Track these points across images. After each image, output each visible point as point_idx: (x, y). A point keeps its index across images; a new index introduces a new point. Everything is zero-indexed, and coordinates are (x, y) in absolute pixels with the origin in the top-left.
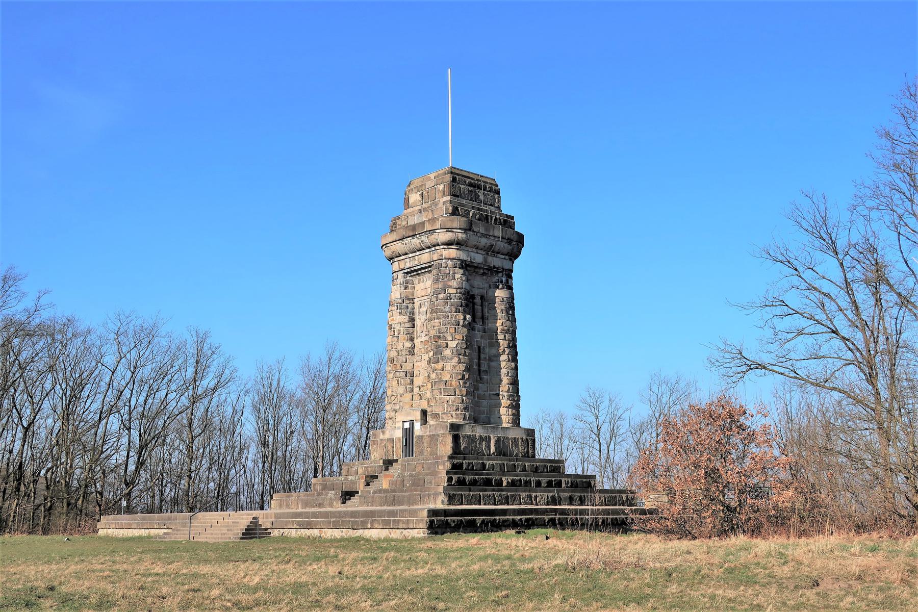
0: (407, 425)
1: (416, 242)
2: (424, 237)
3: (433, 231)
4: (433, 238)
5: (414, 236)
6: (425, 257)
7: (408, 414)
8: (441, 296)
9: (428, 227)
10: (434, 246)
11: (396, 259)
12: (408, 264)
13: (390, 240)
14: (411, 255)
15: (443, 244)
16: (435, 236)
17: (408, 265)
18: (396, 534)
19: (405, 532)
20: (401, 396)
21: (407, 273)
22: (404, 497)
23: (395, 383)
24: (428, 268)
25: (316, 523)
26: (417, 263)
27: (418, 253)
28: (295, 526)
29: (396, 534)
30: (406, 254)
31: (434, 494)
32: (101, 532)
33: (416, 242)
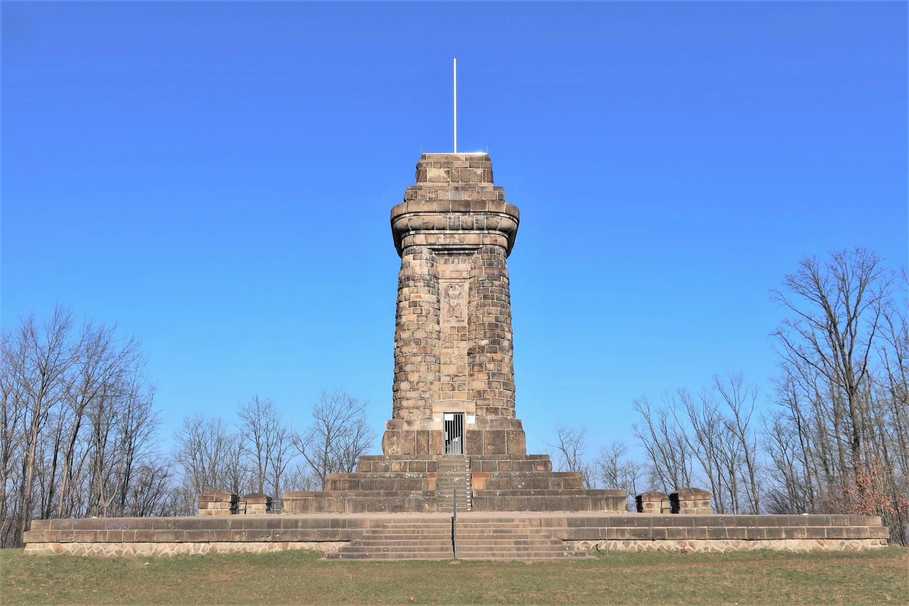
0: (450, 418)
1: (468, 219)
2: (481, 217)
3: (497, 214)
4: (494, 221)
5: (464, 213)
6: (472, 238)
7: (453, 405)
8: (497, 283)
9: (490, 207)
10: (488, 229)
11: (422, 232)
12: (442, 240)
13: (426, 209)
14: (448, 232)
15: (500, 230)
16: (497, 219)
17: (442, 240)
18: (834, 545)
19: (847, 543)
20: (431, 383)
21: (434, 250)
22: (562, 500)
23: (423, 368)
24: (467, 251)
25: (678, 532)
26: (457, 241)
27: (460, 232)
28: (627, 536)
29: (834, 545)
30: (444, 229)
31: (613, 498)
32: (32, 548)
33: (468, 219)
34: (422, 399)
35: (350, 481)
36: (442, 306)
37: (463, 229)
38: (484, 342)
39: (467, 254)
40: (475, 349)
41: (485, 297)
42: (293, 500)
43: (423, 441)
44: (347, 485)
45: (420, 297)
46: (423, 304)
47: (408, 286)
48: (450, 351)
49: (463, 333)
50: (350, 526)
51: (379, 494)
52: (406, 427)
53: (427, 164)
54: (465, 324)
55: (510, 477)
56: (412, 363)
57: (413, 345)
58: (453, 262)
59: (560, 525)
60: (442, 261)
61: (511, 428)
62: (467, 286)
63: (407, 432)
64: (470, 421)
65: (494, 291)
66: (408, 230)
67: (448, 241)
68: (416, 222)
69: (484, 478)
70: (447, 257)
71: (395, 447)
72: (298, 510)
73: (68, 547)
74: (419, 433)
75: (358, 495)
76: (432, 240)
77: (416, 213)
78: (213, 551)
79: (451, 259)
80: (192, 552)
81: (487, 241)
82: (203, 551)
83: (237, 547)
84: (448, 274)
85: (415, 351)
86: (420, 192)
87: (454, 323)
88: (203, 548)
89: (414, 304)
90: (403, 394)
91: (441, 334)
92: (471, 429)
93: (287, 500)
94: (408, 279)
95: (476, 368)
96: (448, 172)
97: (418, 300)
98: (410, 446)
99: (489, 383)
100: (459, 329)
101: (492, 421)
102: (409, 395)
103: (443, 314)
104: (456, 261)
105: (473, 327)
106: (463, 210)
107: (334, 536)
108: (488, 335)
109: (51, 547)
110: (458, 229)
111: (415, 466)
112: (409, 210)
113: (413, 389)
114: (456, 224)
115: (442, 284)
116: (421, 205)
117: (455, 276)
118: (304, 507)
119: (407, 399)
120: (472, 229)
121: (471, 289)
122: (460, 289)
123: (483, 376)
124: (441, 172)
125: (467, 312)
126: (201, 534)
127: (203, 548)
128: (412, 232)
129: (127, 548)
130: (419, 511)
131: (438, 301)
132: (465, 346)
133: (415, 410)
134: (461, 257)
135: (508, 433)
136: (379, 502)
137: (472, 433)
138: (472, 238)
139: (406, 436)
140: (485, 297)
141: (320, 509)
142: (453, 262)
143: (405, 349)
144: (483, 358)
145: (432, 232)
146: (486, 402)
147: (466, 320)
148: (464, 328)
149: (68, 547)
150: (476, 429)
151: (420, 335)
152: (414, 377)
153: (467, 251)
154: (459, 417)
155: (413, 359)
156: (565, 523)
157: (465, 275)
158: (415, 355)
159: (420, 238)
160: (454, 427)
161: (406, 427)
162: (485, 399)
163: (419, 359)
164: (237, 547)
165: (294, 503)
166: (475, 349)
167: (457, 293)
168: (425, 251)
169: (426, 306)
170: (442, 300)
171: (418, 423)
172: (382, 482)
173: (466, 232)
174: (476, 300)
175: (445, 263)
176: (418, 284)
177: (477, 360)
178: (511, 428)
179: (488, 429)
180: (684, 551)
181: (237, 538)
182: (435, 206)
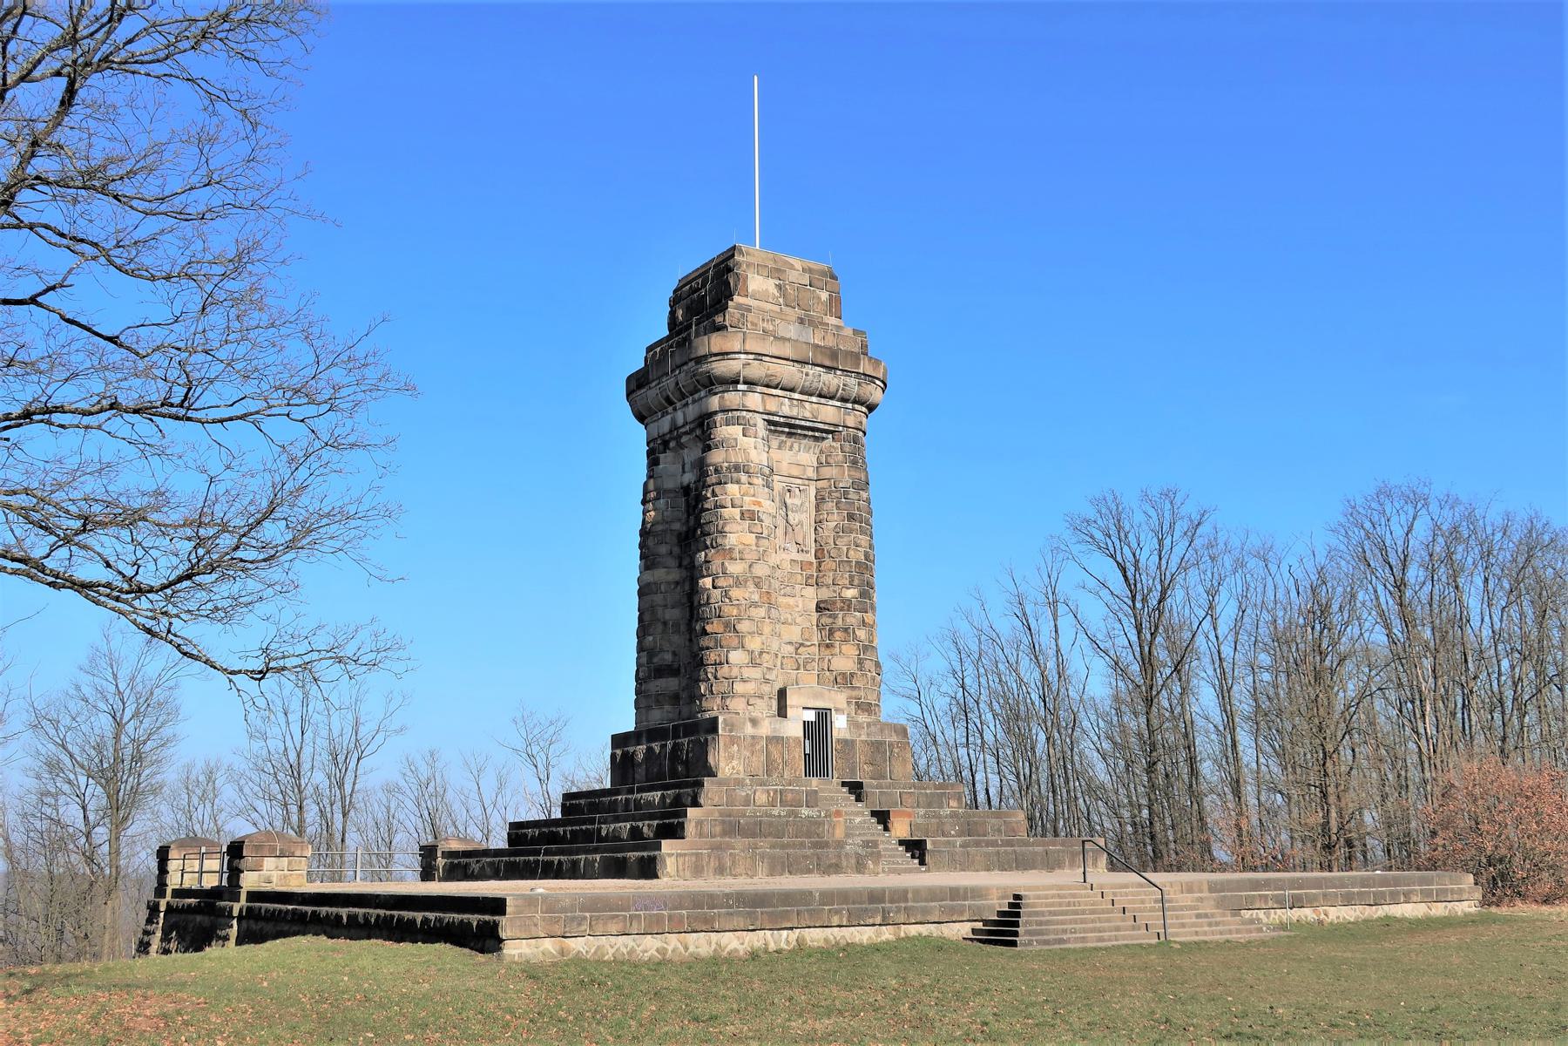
0: (811, 716)
1: (832, 381)
2: (852, 381)
6: (829, 412)
7: (817, 696)
10: (855, 402)
11: (759, 389)
12: (785, 407)
13: (777, 353)
17: (786, 410)
21: (770, 422)
24: (816, 433)
26: (808, 415)
27: (814, 399)
28: (1270, 904)
29: (1439, 910)
30: (792, 390)
33: (832, 381)
34: (767, 681)
35: (723, 822)
37: (820, 396)
38: (850, 593)
39: (816, 439)
40: (834, 603)
41: (851, 517)
42: (678, 855)
43: (776, 754)
44: (718, 829)
45: (759, 504)
46: (763, 517)
47: (738, 482)
48: (791, 601)
50: (973, 898)
51: (802, 845)
52: (749, 730)
53: (748, 265)
55: (939, 817)
56: (750, 618)
57: (752, 588)
59: (1201, 891)
61: (894, 738)
63: (753, 737)
64: (840, 723)
65: (848, 504)
66: (737, 382)
67: (794, 413)
68: (756, 370)
69: (907, 820)
70: (783, 438)
71: (735, 763)
72: (688, 873)
73: (577, 945)
74: (770, 739)
75: (773, 847)
76: (772, 405)
77: (759, 356)
78: (800, 942)
79: (790, 441)
80: (772, 947)
81: (851, 422)
82: (788, 942)
83: (835, 934)
85: (756, 597)
86: (751, 317)
88: (784, 939)
89: (750, 516)
90: (735, 672)
92: (841, 736)
93: (670, 855)
94: (737, 468)
95: (838, 635)
96: (779, 287)
97: (756, 508)
98: (759, 762)
99: (860, 662)
100: (803, 565)
101: (869, 725)
102: (747, 673)
104: (796, 446)
106: (827, 363)
107: (962, 913)
108: (856, 582)
109: (549, 945)
110: (811, 395)
111: (790, 796)
112: (748, 348)
113: (754, 663)
114: (815, 385)
116: (768, 343)
118: (696, 867)
119: (743, 680)
120: (832, 398)
123: (851, 650)
124: (770, 285)
126: (785, 916)
127: (784, 939)
128: (740, 387)
129: (673, 942)
130: (859, 872)
132: (811, 596)
133: (758, 701)
134: (805, 441)
135: (891, 745)
136: (806, 857)
137: (845, 742)
138: (829, 412)
139: (753, 745)
140: (851, 517)
141: (721, 870)
143: (735, 593)
144: (849, 620)
145: (774, 392)
146: (854, 693)
149: (577, 945)
150: (848, 737)
151: (760, 570)
152: (754, 644)
153: (816, 433)
154: (823, 716)
155: (754, 612)
156: (1205, 887)
157: (811, 473)
158: (754, 605)
159: (754, 400)
160: (818, 730)
161: (749, 730)
162: (854, 688)
163: (762, 612)
164: (835, 934)
165: (681, 860)
166: (834, 603)
168: (761, 424)
169: (767, 521)
171: (766, 722)
172: (770, 824)
173: (823, 400)
174: (834, 519)
176: (755, 481)
177: (839, 622)
178: (894, 738)
179: (864, 738)
180: (1321, 922)
181: (835, 920)
182: (787, 351)
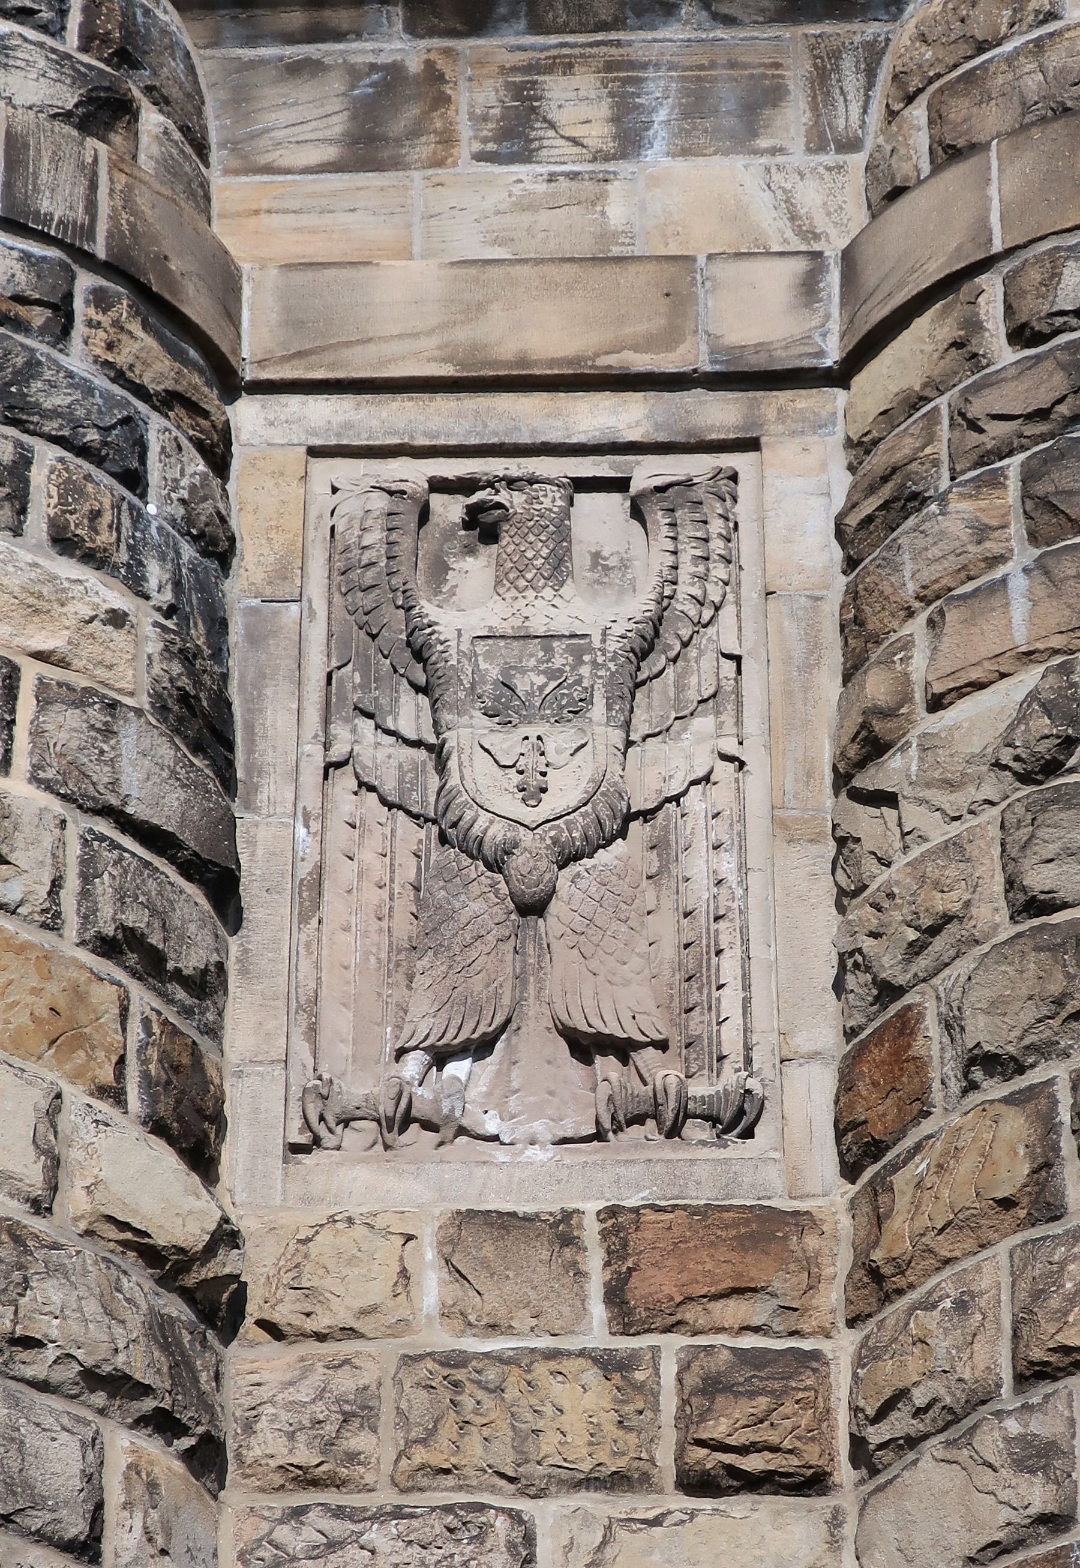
36: (268, 842)
49: (732, 1330)
54: (795, 1159)
58: (516, 133)
60: (304, 119)
62: (796, 491)
84: (403, 316)
87: (527, 1142)
91: (254, 1375)
103: (311, 980)
104: (576, 105)
105: (972, 1142)
115: (291, 485)
117: (549, 334)
121: (881, 510)
122: (647, 555)
125: (821, 932)
131: (203, 722)
142: (516, 133)
147: (806, 1103)
148: (768, 1229)
157: (757, 312)
167: (601, 614)
170: (279, 726)
175: (366, 149)
